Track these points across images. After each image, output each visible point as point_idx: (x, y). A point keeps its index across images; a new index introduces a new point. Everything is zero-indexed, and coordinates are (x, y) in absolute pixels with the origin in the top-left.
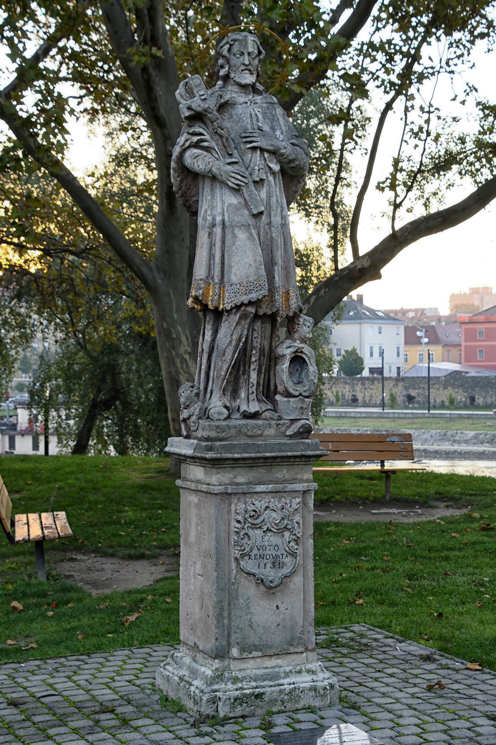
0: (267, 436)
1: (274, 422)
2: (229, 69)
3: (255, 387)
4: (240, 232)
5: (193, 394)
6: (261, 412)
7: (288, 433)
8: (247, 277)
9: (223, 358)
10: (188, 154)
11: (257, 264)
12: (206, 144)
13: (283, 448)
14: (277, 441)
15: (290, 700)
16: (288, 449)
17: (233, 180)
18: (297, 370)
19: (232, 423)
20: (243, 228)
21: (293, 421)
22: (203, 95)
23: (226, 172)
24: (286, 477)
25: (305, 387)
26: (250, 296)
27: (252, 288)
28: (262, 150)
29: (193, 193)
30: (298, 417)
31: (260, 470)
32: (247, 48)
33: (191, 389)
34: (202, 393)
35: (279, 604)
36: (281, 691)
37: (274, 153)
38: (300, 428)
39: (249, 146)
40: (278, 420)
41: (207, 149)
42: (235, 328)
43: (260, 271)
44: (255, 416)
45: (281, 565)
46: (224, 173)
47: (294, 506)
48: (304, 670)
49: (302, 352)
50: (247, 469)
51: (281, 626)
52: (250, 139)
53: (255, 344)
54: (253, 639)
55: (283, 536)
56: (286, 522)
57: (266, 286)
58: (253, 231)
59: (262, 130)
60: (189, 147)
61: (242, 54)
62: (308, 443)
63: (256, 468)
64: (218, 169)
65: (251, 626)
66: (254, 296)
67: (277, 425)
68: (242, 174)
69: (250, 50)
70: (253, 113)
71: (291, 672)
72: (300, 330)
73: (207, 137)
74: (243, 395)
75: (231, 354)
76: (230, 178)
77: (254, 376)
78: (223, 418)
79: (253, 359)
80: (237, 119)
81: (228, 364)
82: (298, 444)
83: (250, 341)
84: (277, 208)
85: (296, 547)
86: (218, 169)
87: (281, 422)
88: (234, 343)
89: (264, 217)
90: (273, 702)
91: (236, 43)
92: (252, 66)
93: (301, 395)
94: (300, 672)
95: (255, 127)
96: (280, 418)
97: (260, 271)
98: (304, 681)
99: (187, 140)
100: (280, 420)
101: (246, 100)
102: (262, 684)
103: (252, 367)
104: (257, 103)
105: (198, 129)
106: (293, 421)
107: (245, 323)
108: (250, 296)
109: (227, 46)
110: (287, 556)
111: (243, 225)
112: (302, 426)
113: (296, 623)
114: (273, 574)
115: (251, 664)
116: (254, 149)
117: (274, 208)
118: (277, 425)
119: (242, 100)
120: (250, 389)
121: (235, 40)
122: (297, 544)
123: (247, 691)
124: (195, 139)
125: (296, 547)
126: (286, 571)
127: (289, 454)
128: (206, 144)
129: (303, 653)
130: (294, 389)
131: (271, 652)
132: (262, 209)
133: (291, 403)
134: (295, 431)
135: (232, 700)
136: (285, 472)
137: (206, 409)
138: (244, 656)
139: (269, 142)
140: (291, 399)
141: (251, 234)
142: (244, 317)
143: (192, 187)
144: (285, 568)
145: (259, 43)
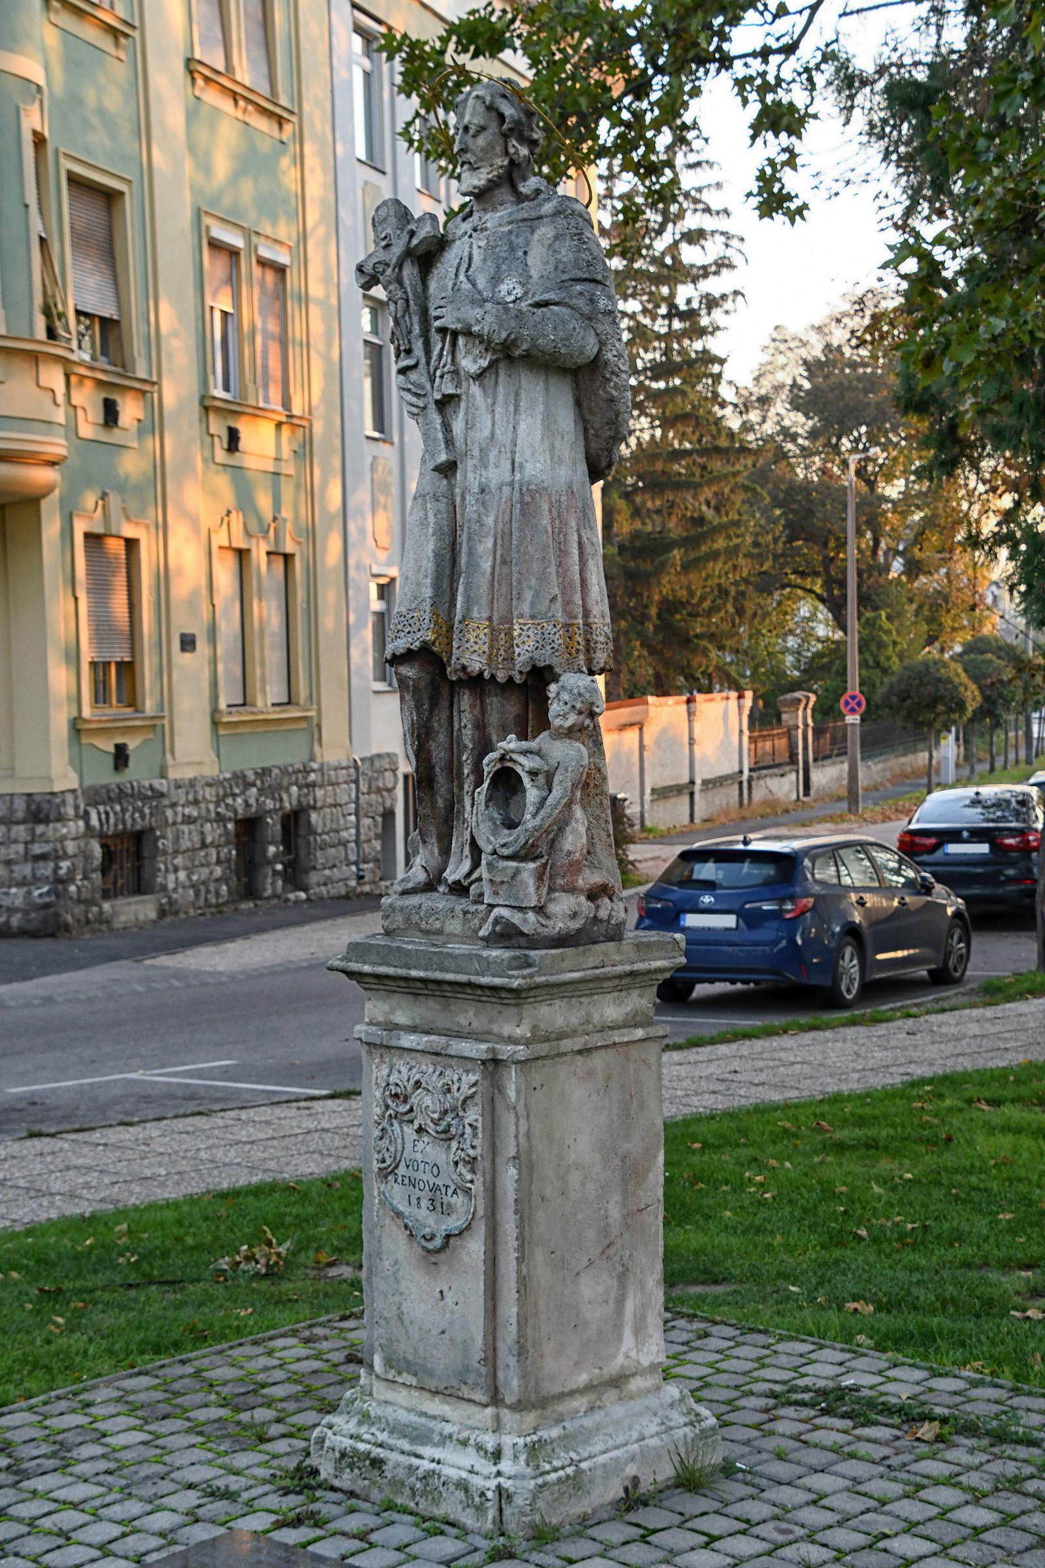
0: (449, 935)
15: (425, 1493)
24: (474, 1025)
31: (431, 1003)
35: (445, 1289)
36: (410, 1467)
45: (447, 1210)
47: (466, 1091)
48: (472, 1442)
49: (511, 760)
51: (447, 1336)
54: (404, 1348)
55: (449, 1147)
56: (448, 1119)
62: (486, 960)
63: (423, 999)
65: (400, 1317)
67: (465, 913)
71: (450, 1436)
85: (469, 1177)
90: (397, 1484)
94: (464, 1443)
98: (456, 1463)
102: (392, 1442)
110: (455, 1192)
113: (473, 1340)
114: (432, 1223)
115: (401, 1397)
117: (476, 452)
122: (473, 1171)
123: (362, 1447)
125: (469, 1177)
126: (454, 1223)
127: (450, 977)
129: (486, 1406)
131: (432, 1384)
135: (337, 1455)
136: (471, 1013)
138: (390, 1377)
144: (454, 1216)
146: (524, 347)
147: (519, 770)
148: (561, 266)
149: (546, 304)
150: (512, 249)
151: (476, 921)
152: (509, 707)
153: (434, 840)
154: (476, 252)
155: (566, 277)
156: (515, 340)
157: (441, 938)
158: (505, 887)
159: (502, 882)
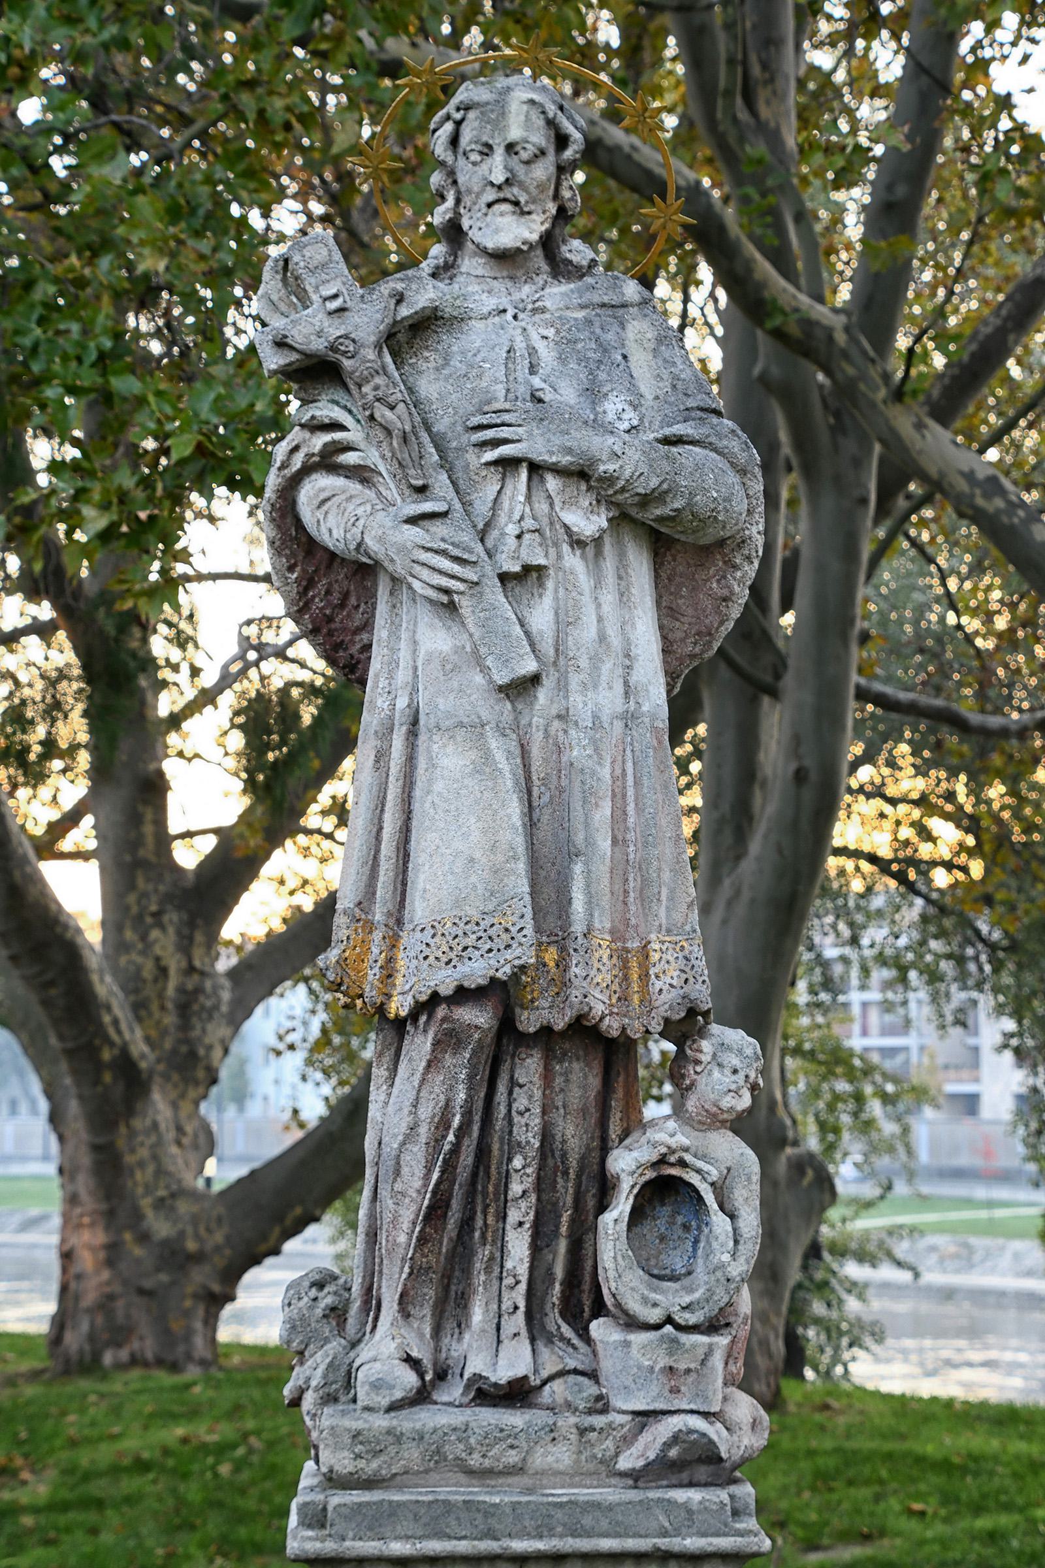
0: (543, 1473)
1: (573, 1420)
2: (458, 201)
3: (523, 1287)
4: (450, 749)
5: (319, 1312)
6: (535, 1381)
7: (625, 1463)
8: (457, 904)
9: (398, 1186)
10: (307, 494)
11: (500, 858)
12: (350, 458)
13: (587, 1521)
14: (584, 1493)
16: (604, 1524)
17: (425, 574)
18: (686, 1227)
19: (427, 1418)
20: (460, 734)
21: (645, 1417)
22: (335, 296)
23: (402, 549)
25: (690, 1290)
26: (465, 969)
27: (471, 940)
28: (536, 469)
29: (358, 619)
30: (660, 1405)
32: (505, 129)
33: (313, 1292)
34: (356, 1306)
37: (580, 473)
38: (667, 1445)
39: (490, 455)
40: (590, 1412)
41: (362, 474)
42: (423, 1081)
43: (510, 881)
44: (517, 1394)
46: (399, 552)
49: (682, 1163)
52: (489, 434)
53: (520, 1134)
57: (529, 931)
58: (494, 743)
59: (540, 401)
60: (307, 470)
61: (487, 150)
62: (686, 1507)
64: (381, 540)
66: (476, 971)
67: (582, 1431)
68: (456, 552)
69: (515, 133)
70: (520, 345)
72: (702, 1081)
73: (355, 434)
74: (478, 1315)
75: (420, 1172)
76: (417, 569)
77: (518, 1247)
78: (385, 1402)
79: (516, 1188)
80: (463, 368)
81: (414, 1208)
82: (646, 1505)
83: (499, 1124)
84: (596, 661)
86: (381, 540)
87: (599, 1421)
88: (424, 1131)
89: (542, 695)
91: (472, 115)
92: (522, 186)
93: (669, 1320)
95: (522, 390)
96: (601, 1405)
97: (510, 881)
99: (296, 449)
100: (605, 1410)
101: (504, 302)
103: (513, 1216)
104: (543, 310)
105: (325, 410)
106: (645, 1417)
107: (458, 1063)
108: (465, 969)
109: (449, 127)
111: (461, 725)
112: (676, 1439)
116: (508, 465)
117: (584, 663)
118: (582, 1431)
119: (491, 303)
120: (506, 1295)
121: (466, 107)
124: (321, 440)
127: (607, 1544)
128: (350, 458)
130: (645, 1300)
132: (530, 666)
133: (634, 1351)
134: (652, 1456)
137: (350, 1365)
139: (557, 440)
140: (639, 1338)
141: (487, 756)
142: (449, 1040)
143: (353, 601)
145: (552, 109)
146: (677, 505)
147: (694, 1179)
148: (680, 385)
149: (677, 441)
151: (609, 1444)
152: (591, 1079)
153: (427, 1311)
154: (541, 346)
155: (691, 403)
156: (666, 492)
157: (525, 1481)
158: (694, 1375)
159: (688, 1371)
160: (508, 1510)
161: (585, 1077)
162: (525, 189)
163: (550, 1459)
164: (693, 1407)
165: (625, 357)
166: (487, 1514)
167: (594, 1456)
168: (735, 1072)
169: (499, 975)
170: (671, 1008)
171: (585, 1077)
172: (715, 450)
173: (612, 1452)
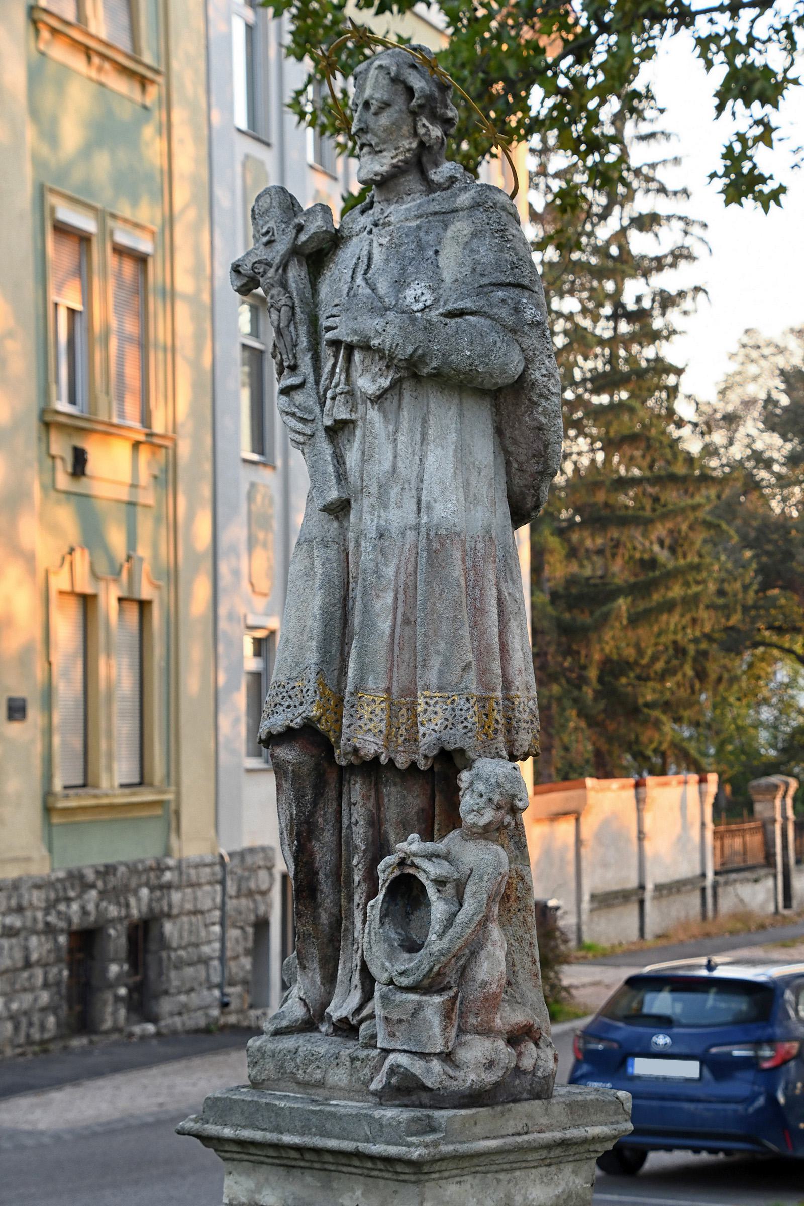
27: (278, 700)
49: (413, 865)
50: (282, 1171)
62: (379, 1121)
63: (297, 1172)
67: (353, 1059)
117: (374, 489)
136: (359, 1193)
146: (434, 364)
147: (422, 877)
149: (461, 313)
150: (421, 248)
151: (367, 1070)
152: (410, 799)
153: (316, 965)
154: (376, 251)
155: (485, 281)
158: (403, 1026)
159: (400, 1021)
160: (288, 1113)
161: (404, 798)
162: (375, 134)
163: (336, 1078)
164: (405, 1047)
165: (437, 252)
166: (278, 1115)
167: (359, 1079)
168: (481, 796)
169: (292, 724)
170: (428, 748)
171: (404, 798)
172: (489, 316)
173: (368, 1077)
